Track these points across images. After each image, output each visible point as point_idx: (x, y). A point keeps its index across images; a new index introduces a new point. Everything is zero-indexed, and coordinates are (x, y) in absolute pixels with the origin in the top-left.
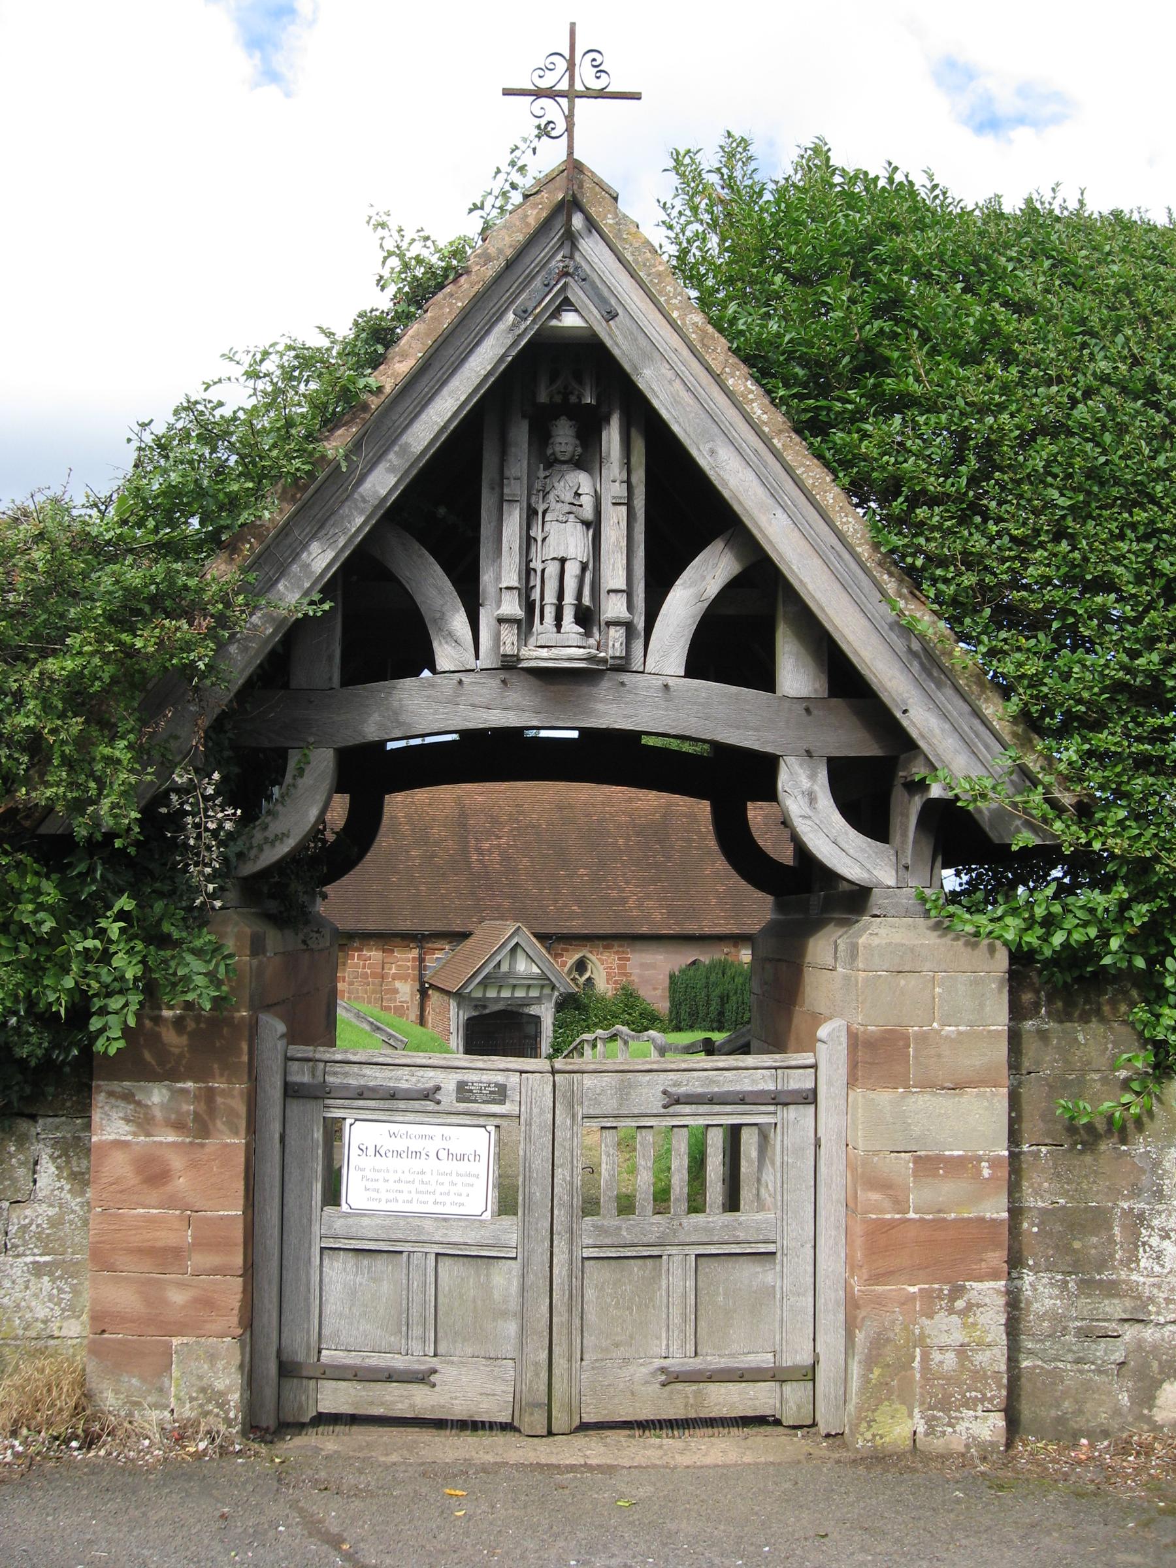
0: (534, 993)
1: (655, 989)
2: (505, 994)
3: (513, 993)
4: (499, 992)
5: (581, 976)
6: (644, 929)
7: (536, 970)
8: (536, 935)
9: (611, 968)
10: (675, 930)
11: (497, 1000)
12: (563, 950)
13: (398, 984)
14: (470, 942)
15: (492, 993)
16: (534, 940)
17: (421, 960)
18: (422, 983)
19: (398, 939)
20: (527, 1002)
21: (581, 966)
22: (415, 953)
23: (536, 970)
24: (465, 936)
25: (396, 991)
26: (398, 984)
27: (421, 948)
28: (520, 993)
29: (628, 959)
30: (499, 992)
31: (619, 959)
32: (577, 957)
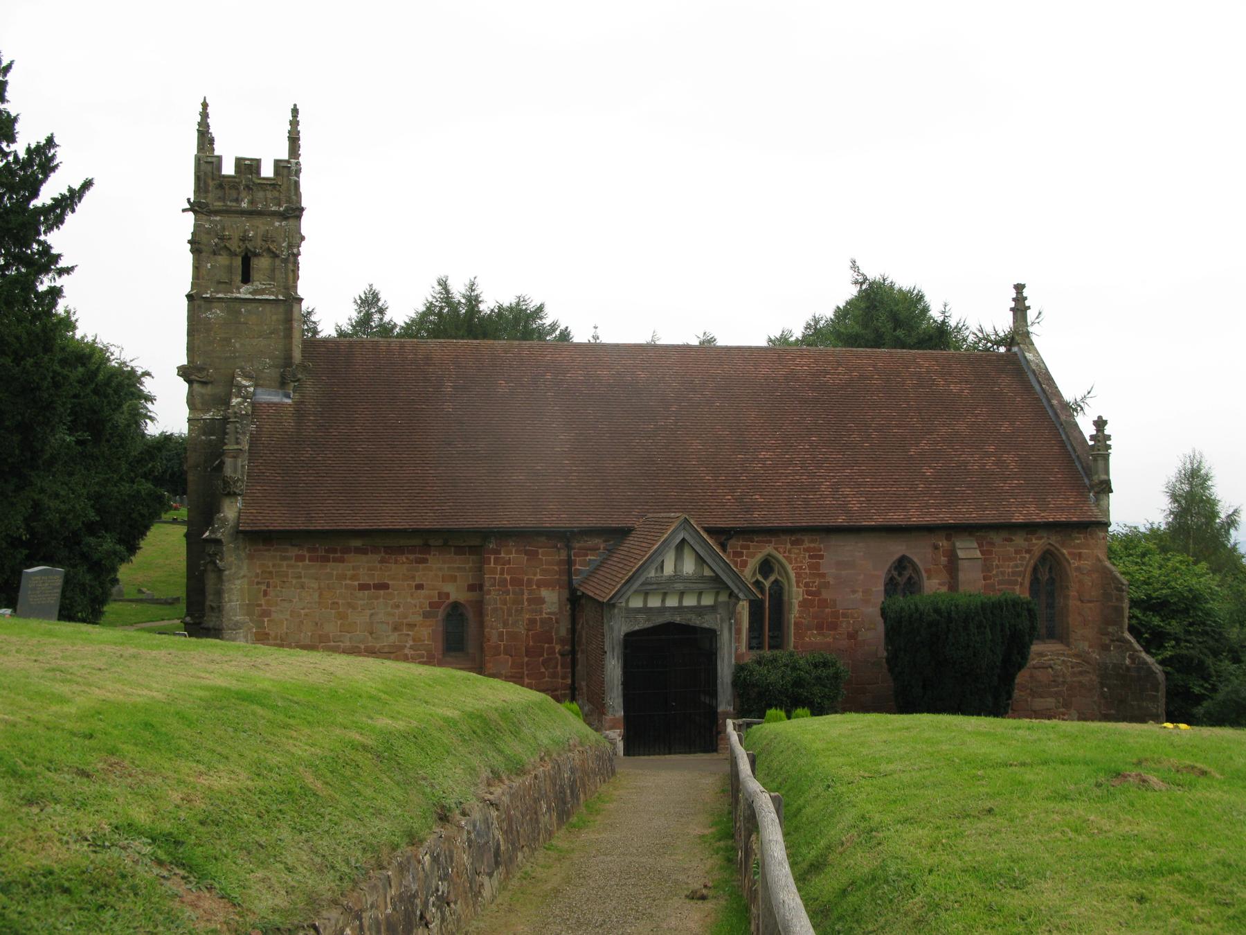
0: (707, 601)
1: (854, 592)
2: (672, 602)
3: (699, 601)
4: (663, 601)
5: (766, 577)
6: (841, 520)
7: (707, 572)
8: (709, 531)
9: (801, 568)
10: (877, 520)
11: (662, 610)
12: (743, 547)
13: (545, 593)
14: (631, 541)
16: (705, 536)
17: (570, 562)
18: (573, 591)
19: (543, 539)
21: (766, 567)
22: (563, 556)
23: (707, 572)
24: (623, 533)
25: (541, 601)
26: (545, 593)
27: (569, 548)
29: (821, 557)
30: (663, 601)
31: (811, 557)
32: (759, 557)
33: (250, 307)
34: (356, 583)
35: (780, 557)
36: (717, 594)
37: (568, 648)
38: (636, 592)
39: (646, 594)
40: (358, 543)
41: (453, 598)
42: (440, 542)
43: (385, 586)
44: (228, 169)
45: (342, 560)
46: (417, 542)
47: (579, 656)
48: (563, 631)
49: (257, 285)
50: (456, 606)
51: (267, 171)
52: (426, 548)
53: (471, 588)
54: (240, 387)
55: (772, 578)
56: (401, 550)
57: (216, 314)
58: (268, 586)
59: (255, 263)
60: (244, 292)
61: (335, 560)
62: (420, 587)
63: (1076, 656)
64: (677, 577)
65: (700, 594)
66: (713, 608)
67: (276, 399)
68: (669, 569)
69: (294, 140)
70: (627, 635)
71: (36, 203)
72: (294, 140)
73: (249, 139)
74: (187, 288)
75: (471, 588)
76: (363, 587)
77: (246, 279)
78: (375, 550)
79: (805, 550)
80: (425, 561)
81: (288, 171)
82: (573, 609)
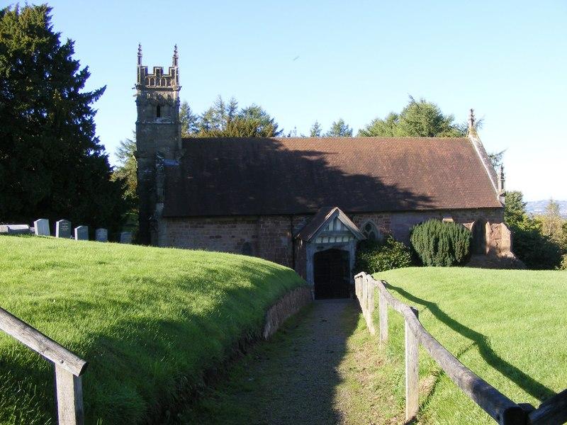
0: (346, 240)
2: (332, 241)
15: (325, 241)
20: (342, 244)
25: (281, 241)
28: (339, 240)
33: (161, 126)
34: (208, 236)
35: (374, 223)
36: (349, 237)
37: (291, 259)
38: (319, 237)
39: (323, 238)
40: (208, 220)
41: (246, 241)
42: (241, 219)
43: (218, 237)
44: (150, 71)
45: (203, 227)
46: (232, 219)
47: (296, 262)
48: (290, 251)
49: (163, 118)
50: (247, 244)
51: (166, 72)
52: (236, 221)
53: (253, 237)
54: (159, 159)
55: (371, 231)
56: (225, 223)
57: (147, 130)
58: (175, 237)
59: (162, 109)
60: (158, 121)
61: (200, 227)
62: (233, 237)
63: (491, 261)
64: (334, 231)
65: (343, 238)
66: (348, 243)
67: (172, 163)
68: (331, 228)
69: (175, 59)
70: (316, 254)
71: (81, 91)
72: (175, 59)
73: (157, 60)
74: (136, 119)
75: (253, 237)
76: (211, 237)
77: (159, 116)
78: (216, 223)
79: (384, 220)
80: (235, 226)
81: (174, 74)
82: (293, 244)
